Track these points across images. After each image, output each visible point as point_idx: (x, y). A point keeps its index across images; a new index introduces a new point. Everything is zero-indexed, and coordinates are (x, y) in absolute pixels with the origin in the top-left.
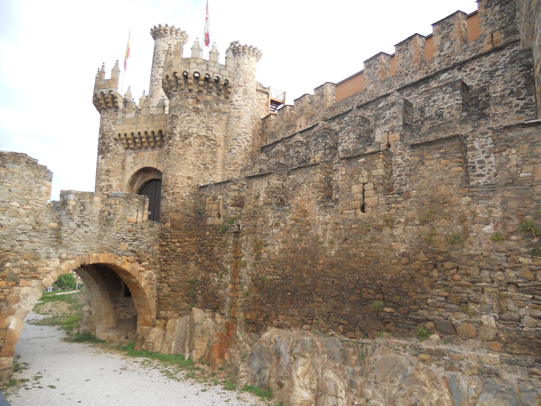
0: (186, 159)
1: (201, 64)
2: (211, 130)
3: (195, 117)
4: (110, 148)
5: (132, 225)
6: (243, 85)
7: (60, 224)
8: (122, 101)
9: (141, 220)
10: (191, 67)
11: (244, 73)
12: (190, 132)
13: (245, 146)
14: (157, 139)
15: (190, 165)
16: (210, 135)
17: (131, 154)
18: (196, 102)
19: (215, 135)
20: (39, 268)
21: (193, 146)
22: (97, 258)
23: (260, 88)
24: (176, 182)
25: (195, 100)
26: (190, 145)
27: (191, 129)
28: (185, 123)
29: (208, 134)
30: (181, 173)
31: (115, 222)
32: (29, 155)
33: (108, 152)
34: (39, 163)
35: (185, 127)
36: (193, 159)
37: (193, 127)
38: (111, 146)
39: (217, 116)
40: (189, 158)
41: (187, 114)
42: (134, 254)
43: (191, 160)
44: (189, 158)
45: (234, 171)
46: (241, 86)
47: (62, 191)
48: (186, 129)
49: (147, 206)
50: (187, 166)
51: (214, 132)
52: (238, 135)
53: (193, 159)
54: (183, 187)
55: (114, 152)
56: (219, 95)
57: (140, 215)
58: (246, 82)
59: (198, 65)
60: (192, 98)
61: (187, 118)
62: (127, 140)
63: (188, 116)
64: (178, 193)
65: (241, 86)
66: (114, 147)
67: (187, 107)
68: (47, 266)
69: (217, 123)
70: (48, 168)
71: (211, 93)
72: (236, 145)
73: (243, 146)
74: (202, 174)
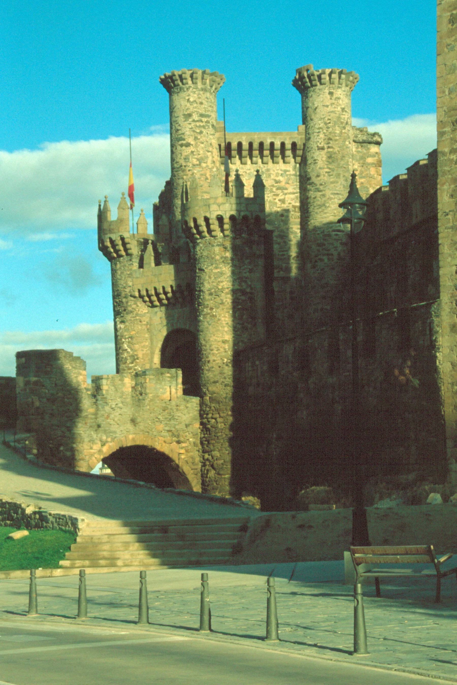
0: (219, 320)
1: (223, 204)
2: (246, 282)
3: (224, 269)
4: (130, 309)
5: (165, 403)
6: (326, 146)
7: (97, 409)
8: (136, 243)
9: (175, 395)
10: (211, 209)
11: (326, 124)
12: (220, 287)
13: (339, 254)
14: (186, 293)
15: (224, 327)
16: (244, 287)
17: (156, 312)
18: (222, 249)
19: (250, 286)
20: (85, 451)
21: (226, 303)
22: (133, 439)
23: (361, 138)
24: (211, 348)
25: (222, 247)
26: (222, 303)
27: (222, 284)
28: (213, 278)
29: (242, 286)
30: (215, 338)
31: (147, 402)
32: (65, 349)
33: (127, 314)
34: (75, 355)
35: (213, 282)
36: (227, 319)
37: (222, 282)
38: (131, 305)
39: (250, 263)
40: (223, 319)
41: (214, 265)
42: (171, 434)
43: (225, 321)
44: (223, 319)
45: (324, 298)
46: (323, 149)
47: (92, 377)
48: (215, 284)
49: (180, 380)
50: (220, 328)
51: (250, 283)
52: (326, 235)
53: (227, 319)
54: (219, 353)
55: (135, 313)
56: (251, 234)
57: (173, 390)
58: (331, 139)
59: (219, 206)
60: (218, 245)
61: (216, 271)
62: (149, 296)
63: (216, 268)
64: (214, 361)
65: (323, 149)
66: (134, 306)
67: (213, 258)
68: (91, 448)
69: (251, 271)
70: (81, 358)
71: (240, 235)
72: (324, 255)
73: (335, 253)
74: (241, 336)
